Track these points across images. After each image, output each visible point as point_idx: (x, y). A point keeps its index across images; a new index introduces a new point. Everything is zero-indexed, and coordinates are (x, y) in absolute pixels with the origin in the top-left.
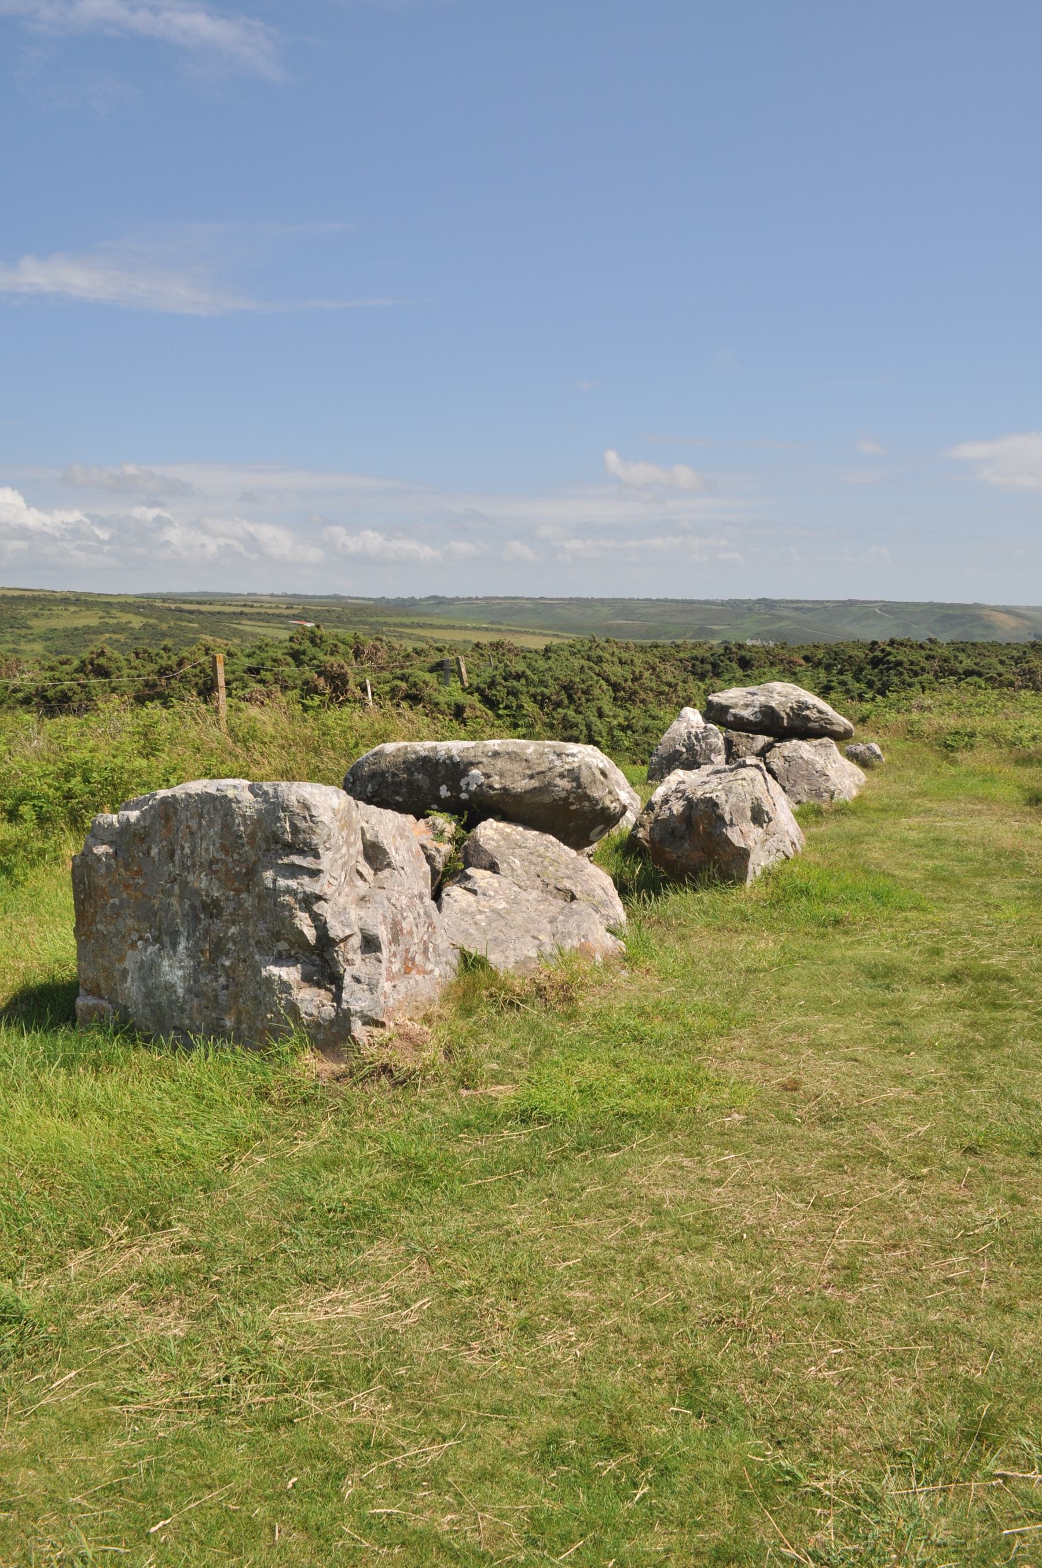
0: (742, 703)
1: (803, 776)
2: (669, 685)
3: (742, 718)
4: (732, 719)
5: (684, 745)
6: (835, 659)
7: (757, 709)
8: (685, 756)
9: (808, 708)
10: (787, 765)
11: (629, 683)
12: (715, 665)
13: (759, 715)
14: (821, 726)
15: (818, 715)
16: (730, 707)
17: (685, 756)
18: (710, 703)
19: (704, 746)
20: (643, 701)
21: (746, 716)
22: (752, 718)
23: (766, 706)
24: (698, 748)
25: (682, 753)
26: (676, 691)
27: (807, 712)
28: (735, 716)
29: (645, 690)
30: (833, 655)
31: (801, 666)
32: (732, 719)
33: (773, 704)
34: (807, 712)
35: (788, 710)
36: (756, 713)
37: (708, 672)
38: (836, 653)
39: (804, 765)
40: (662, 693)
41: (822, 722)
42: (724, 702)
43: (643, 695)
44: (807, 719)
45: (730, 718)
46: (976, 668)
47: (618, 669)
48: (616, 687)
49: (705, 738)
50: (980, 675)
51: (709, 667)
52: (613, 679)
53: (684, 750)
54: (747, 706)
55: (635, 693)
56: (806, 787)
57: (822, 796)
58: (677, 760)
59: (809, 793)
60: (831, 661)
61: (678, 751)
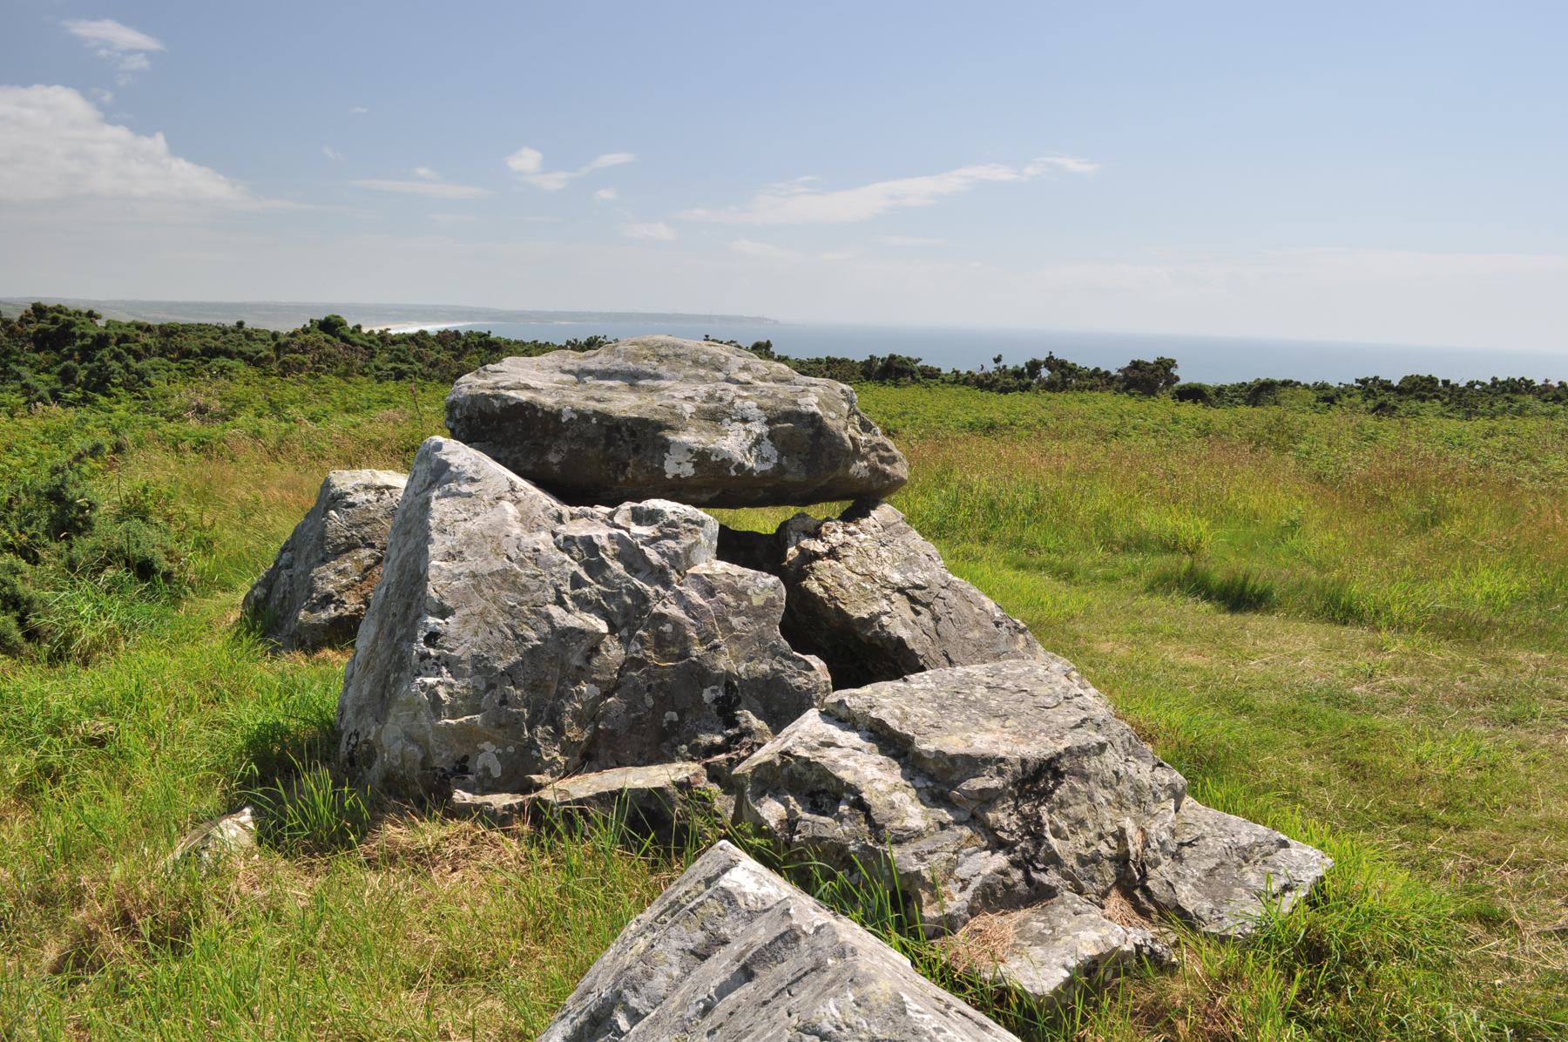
3: (726, 462)
4: (688, 470)
5: (585, 604)
7: (758, 428)
8: (614, 652)
10: (926, 618)
13: (768, 448)
14: (873, 469)
16: (660, 426)
17: (614, 652)
19: (695, 597)
21: (738, 456)
23: (787, 416)
24: (674, 611)
25: (594, 644)
28: (702, 457)
32: (688, 470)
45: (676, 467)
46: (218, 344)
53: (603, 627)
54: (715, 416)
58: (581, 673)
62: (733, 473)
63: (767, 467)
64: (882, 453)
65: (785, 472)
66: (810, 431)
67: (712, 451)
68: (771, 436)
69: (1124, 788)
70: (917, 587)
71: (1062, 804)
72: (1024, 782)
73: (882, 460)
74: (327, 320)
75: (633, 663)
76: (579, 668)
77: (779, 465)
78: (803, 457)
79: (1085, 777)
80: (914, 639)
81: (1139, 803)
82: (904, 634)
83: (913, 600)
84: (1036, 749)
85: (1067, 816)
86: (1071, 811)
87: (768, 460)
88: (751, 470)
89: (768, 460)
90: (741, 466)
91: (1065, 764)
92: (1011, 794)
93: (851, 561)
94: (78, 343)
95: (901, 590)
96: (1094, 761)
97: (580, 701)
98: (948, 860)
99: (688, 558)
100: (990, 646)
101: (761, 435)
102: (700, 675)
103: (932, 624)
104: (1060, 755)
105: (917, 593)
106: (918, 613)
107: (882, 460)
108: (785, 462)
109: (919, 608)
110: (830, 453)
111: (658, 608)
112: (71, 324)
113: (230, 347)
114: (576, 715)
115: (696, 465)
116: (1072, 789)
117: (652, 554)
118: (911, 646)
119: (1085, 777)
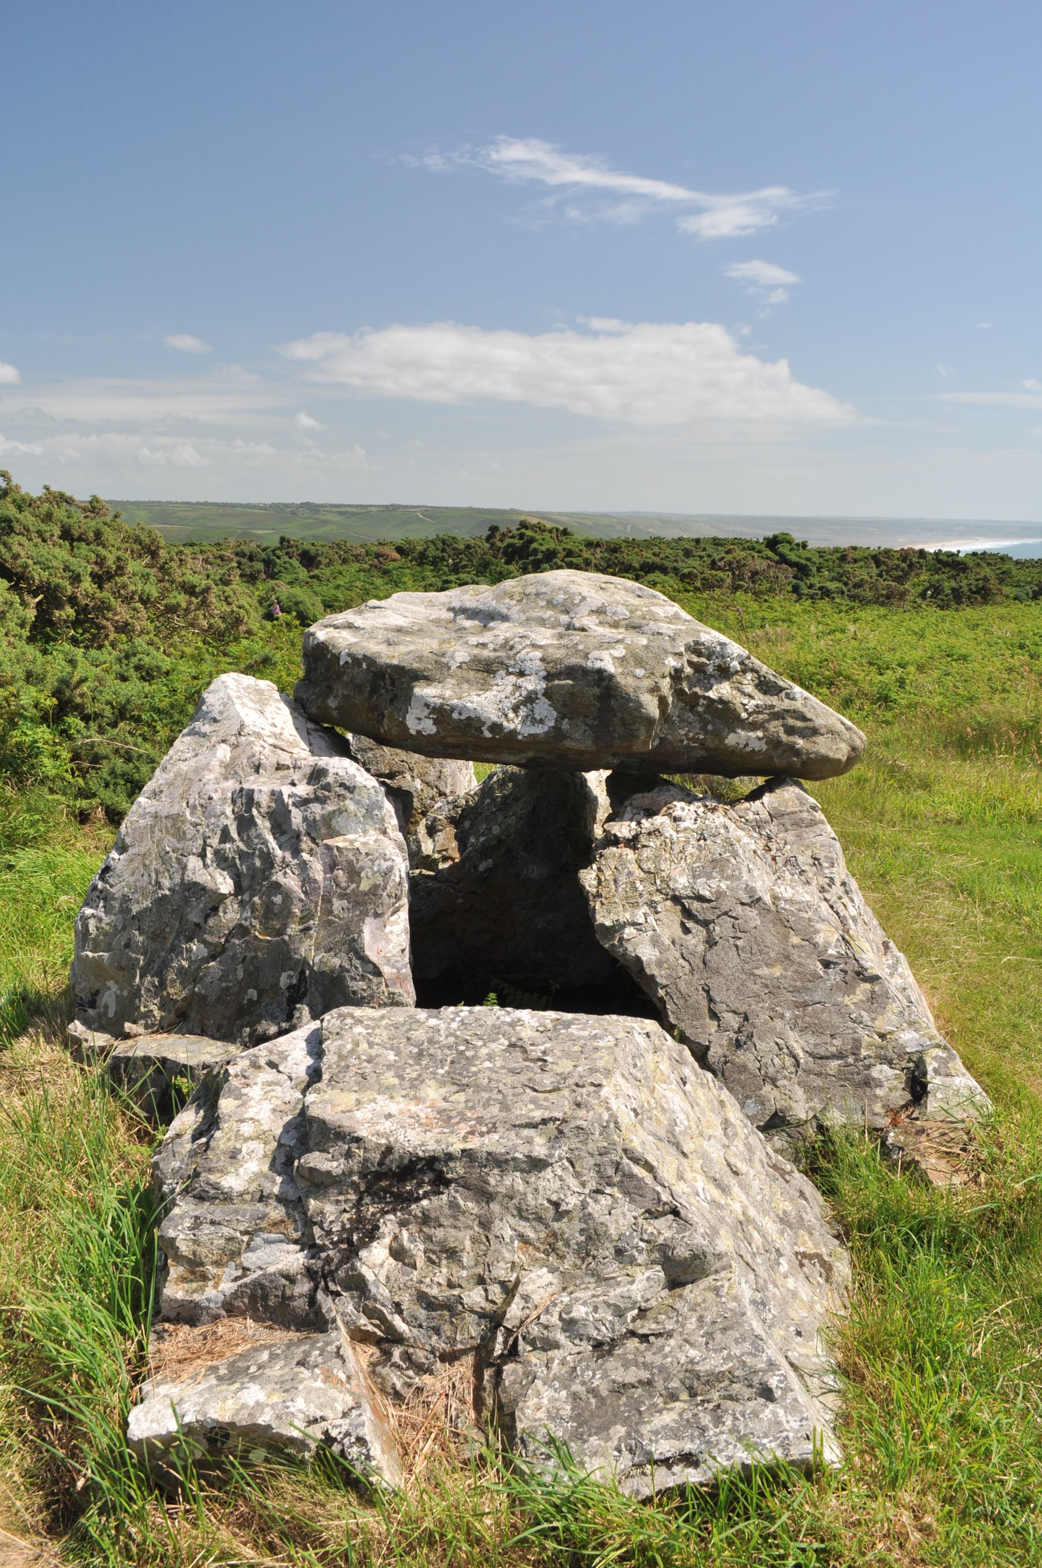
0: (462, 655)
1: (772, 989)
2: (190, 590)
4: (429, 727)
5: (223, 861)
6: (443, 550)
7: (532, 684)
8: (231, 915)
9: (724, 673)
10: (696, 940)
11: (87, 585)
12: (268, 563)
13: (543, 708)
14: (774, 743)
15: (760, 699)
16: (416, 676)
17: (231, 915)
18: (319, 657)
19: (317, 870)
20: (124, 628)
22: (514, 723)
23: (571, 671)
24: (291, 881)
25: (215, 903)
26: (204, 604)
27: (722, 690)
28: (441, 713)
29: (127, 600)
30: (440, 545)
31: (394, 560)
32: (429, 727)
33: (607, 662)
34: (722, 690)
35: (666, 684)
36: (530, 699)
37: (259, 572)
38: (444, 542)
39: (771, 938)
40: (172, 609)
41: (775, 727)
42: (389, 655)
43: (123, 613)
44: (724, 714)
45: (419, 722)
46: (657, 560)
47: (61, 553)
48: (51, 597)
49: (321, 829)
50: (664, 570)
51: (259, 566)
52: (38, 575)
53: (225, 884)
54: (486, 669)
55: (103, 608)
56: (798, 1043)
57: (868, 1083)
58: (196, 931)
59: (812, 1070)
60: (438, 553)
61: (195, 889)
62: (487, 734)
63: (539, 730)
64: (791, 722)
65: (565, 737)
66: (596, 691)
67: (453, 709)
68: (548, 694)
69: (572, 1230)
70: (701, 898)
71: (426, 1219)
72: (379, 1176)
73: (791, 731)
74: (775, 537)
75: (241, 930)
76: (197, 925)
77: (556, 728)
78: (589, 721)
79: (485, 1196)
80: (660, 963)
81: (584, 1252)
82: (647, 953)
83: (687, 913)
84: (416, 1139)
85: (429, 1238)
86: (439, 1233)
87: (541, 721)
88: (513, 733)
89: (541, 721)
90: (496, 727)
91: (458, 1169)
92: (355, 1186)
93: (646, 853)
94: (531, 558)
95: (676, 899)
96: (515, 1180)
97: (189, 959)
98: (231, 1239)
99: (329, 826)
100: (796, 990)
101: (535, 692)
102: (283, 955)
103: (701, 948)
104: (450, 1157)
105: (695, 906)
106: (687, 931)
107: (791, 731)
108: (565, 725)
109: (690, 924)
110: (622, 719)
111: (278, 877)
112: (532, 540)
113: (666, 563)
114: (181, 972)
115: (436, 722)
116: (453, 1205)
117: (297, 817)
118: (652, 970)
119: (485, 1196)
